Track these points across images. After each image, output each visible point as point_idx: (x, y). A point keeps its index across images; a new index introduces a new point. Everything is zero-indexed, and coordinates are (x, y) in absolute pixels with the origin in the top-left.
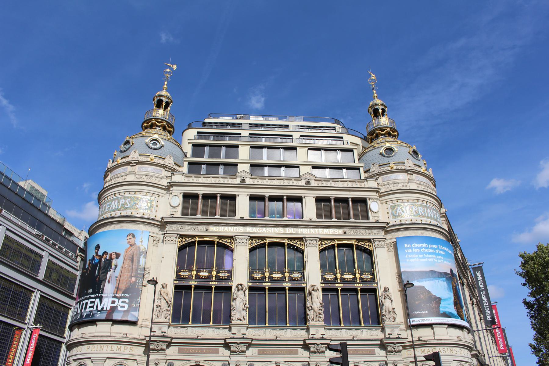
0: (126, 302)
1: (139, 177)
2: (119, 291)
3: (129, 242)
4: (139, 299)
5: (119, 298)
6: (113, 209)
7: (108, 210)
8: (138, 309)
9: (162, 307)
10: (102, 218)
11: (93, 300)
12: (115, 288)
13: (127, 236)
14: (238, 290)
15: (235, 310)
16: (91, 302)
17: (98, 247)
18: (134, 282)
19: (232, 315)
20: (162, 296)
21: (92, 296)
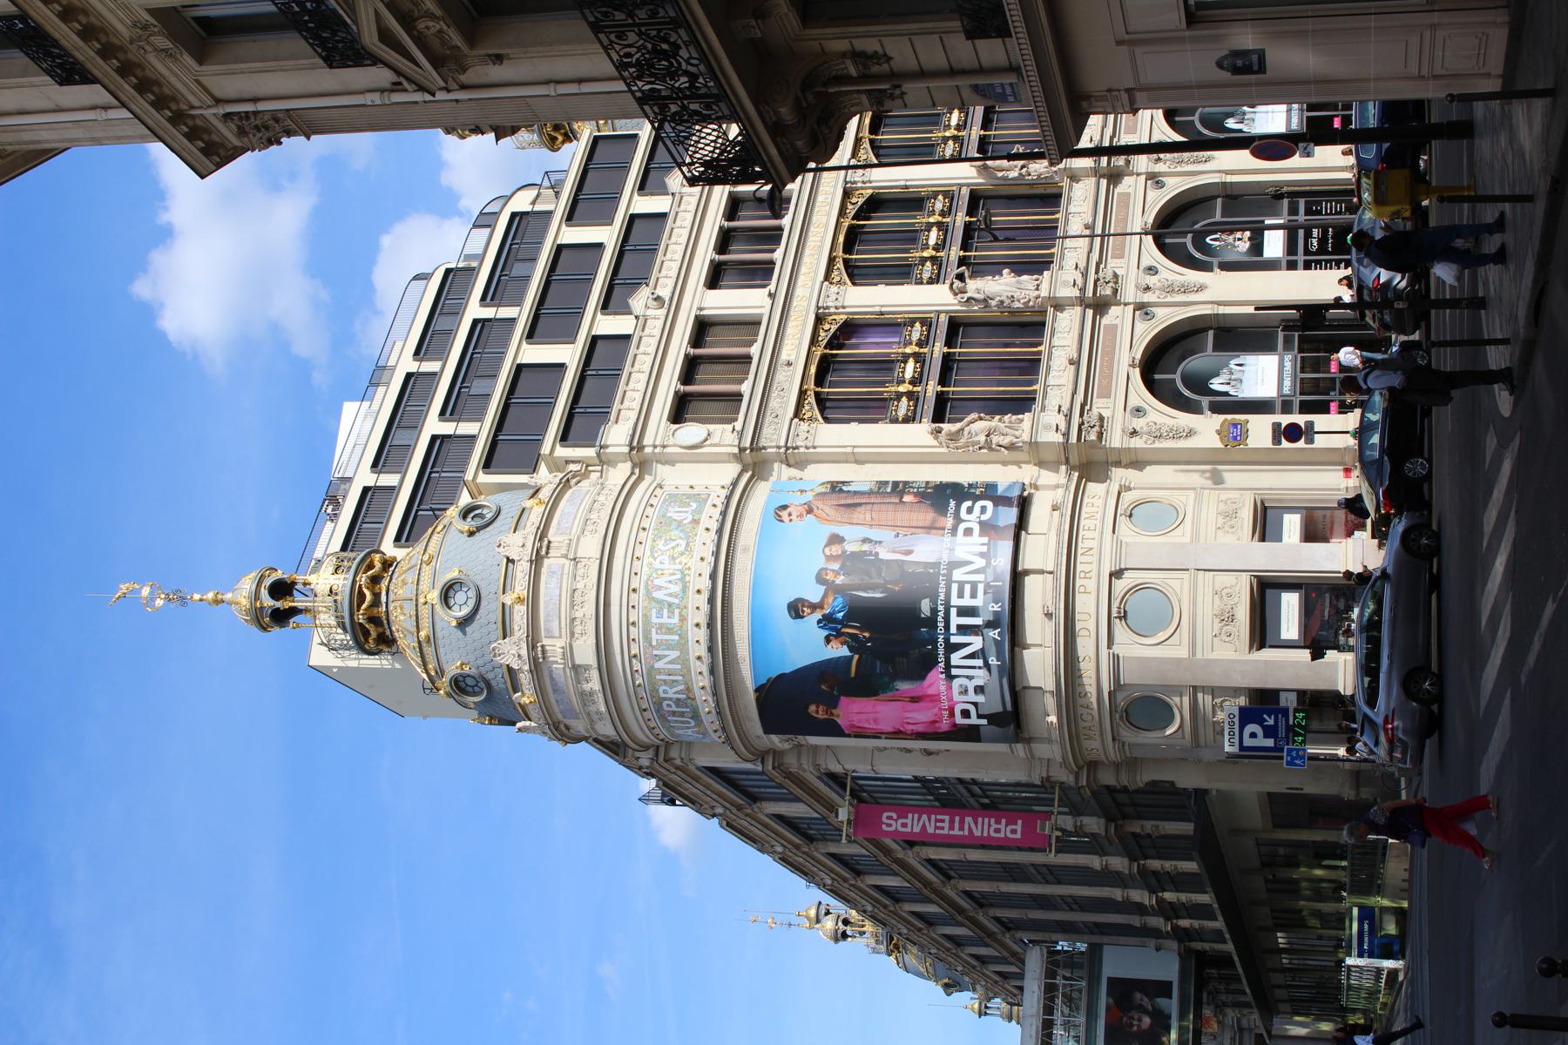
6: (676, 589)
7: (677, 611)
13: (782, 521)
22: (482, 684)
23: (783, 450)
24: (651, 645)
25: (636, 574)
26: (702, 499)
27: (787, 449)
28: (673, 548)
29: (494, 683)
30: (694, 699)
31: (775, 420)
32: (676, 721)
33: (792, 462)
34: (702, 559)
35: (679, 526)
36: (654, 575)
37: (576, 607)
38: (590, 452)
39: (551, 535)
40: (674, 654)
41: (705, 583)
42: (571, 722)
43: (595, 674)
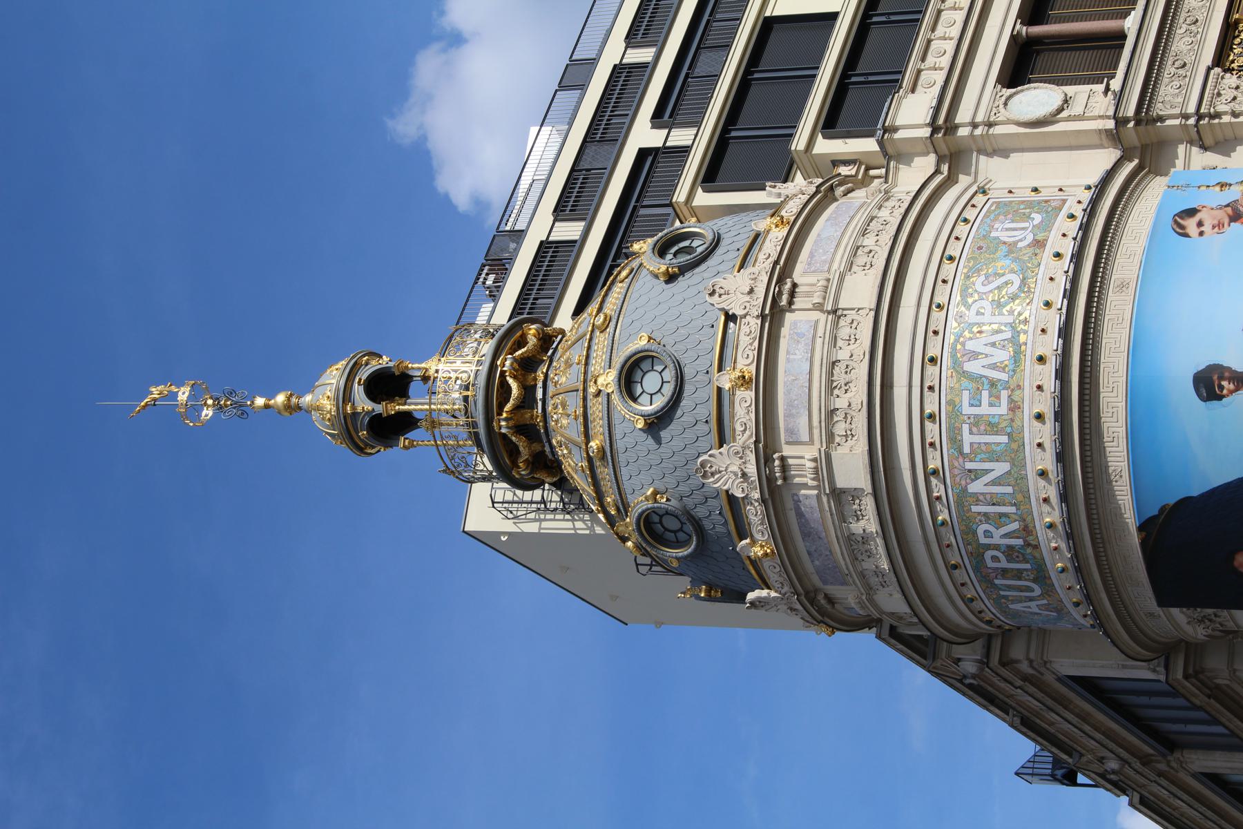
3: (1219, 226)
6: (1003, 356)
7: (1004, 394)
13: (1186, 235)
22: (689, 528)
23: (1192, 121)
24: (961, 453)
25: (936, 333)
26: (1050, 209)
27: (1200, 117)
28: (998, 288)
29: (707, 525)
30: (1037, 547)
31: (1181, 72)
32: (1010, 588)
33: (1208, 141)
34: (1048, 304)
35: (1010, 252)
36: (967, 334)
37: (836, 392)
38: (868, 145)
39: (798, 274)
40: (1001, 468)
41: (1050, 345)
42: (835, 590)
43: (869, 504)
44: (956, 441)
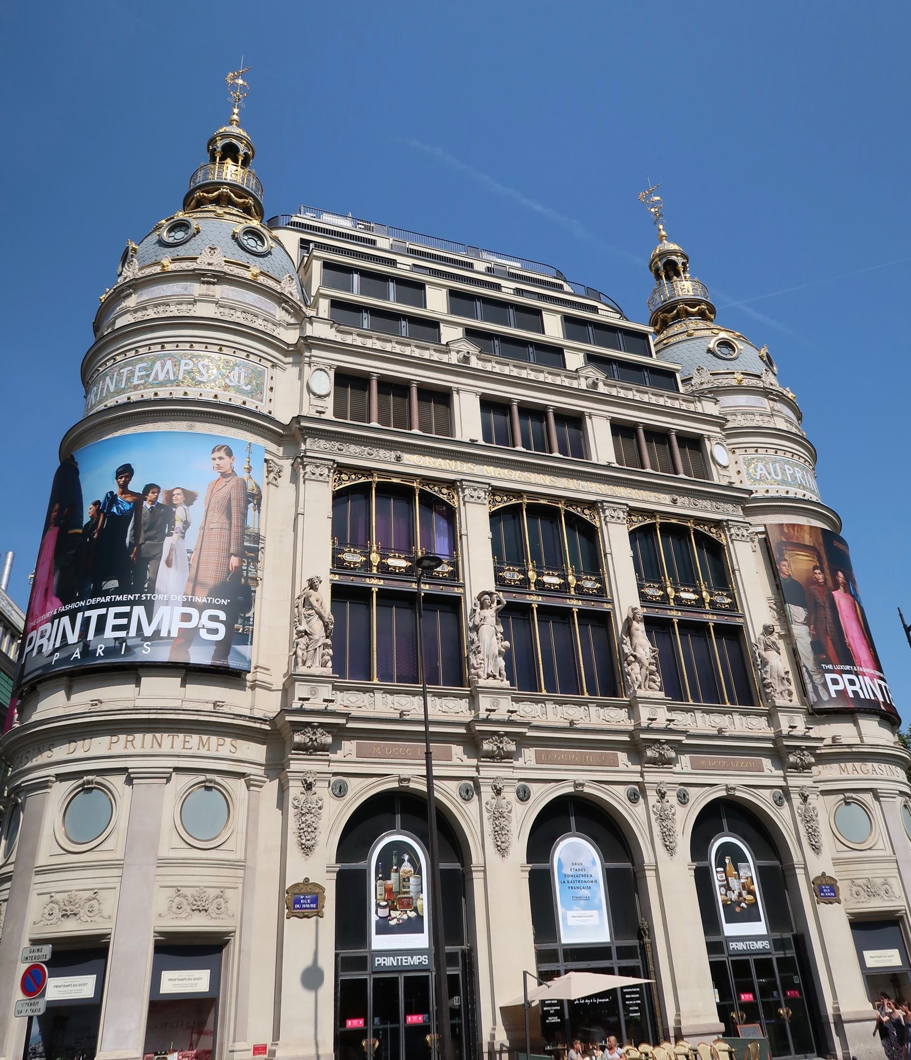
0: (220, 619)
1: (227, 311)
2: (199, 590)
4: (250, 614)
5: (201, 608)
6: (161, 377)
7: (142, 381)
8: (246, 638)
9: (316, 637)
10: (125, 400)
11: (126, 609)
12: (189, 580)
14: (482, 608)
15: (479, 652)
16: (118, 616)
17: (126, 472)
18: (236, 567)
19: (475, 665)
20: (312, 608)
21: (118, 598)
28: (200, 371)
35: (223, 375)
44: (126, 365)
